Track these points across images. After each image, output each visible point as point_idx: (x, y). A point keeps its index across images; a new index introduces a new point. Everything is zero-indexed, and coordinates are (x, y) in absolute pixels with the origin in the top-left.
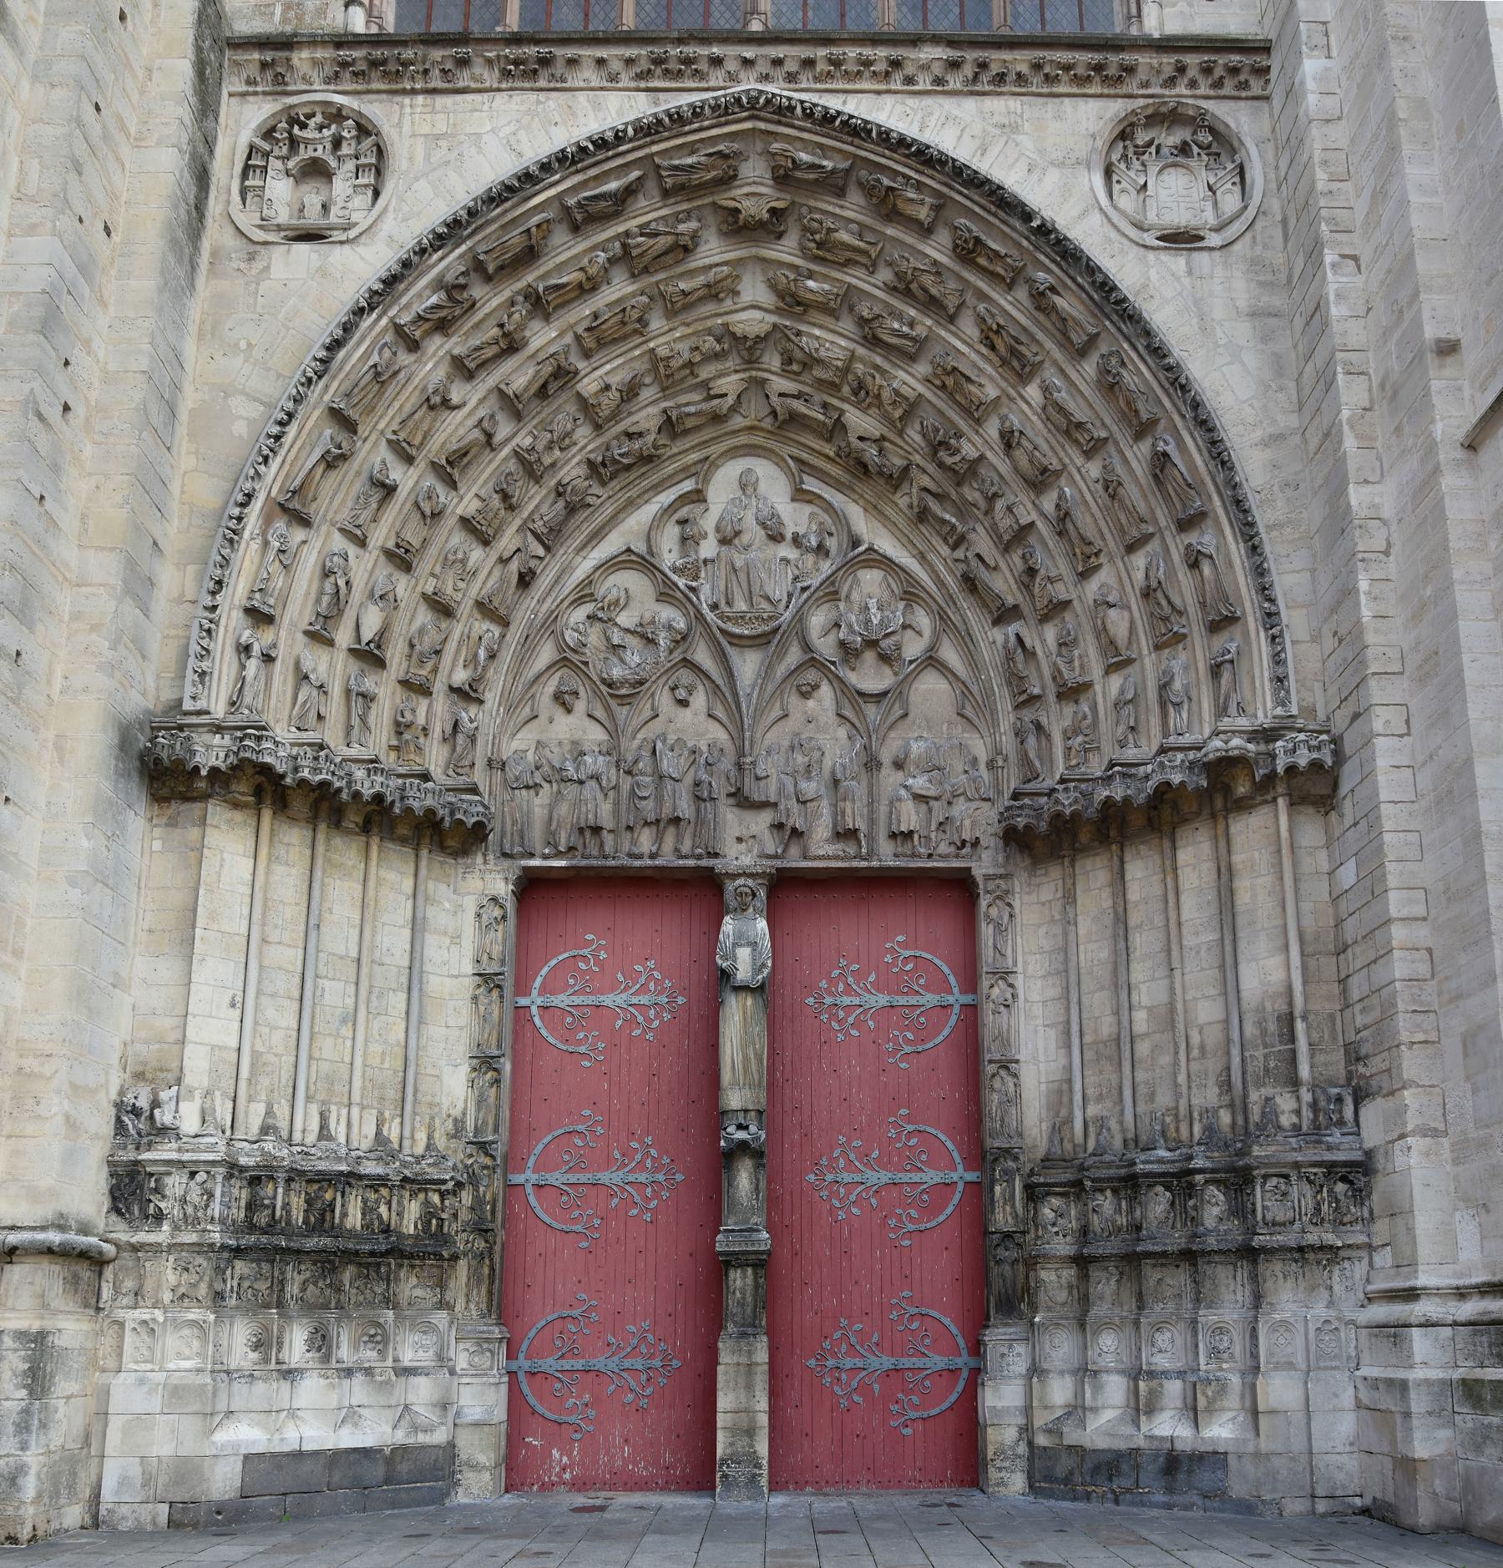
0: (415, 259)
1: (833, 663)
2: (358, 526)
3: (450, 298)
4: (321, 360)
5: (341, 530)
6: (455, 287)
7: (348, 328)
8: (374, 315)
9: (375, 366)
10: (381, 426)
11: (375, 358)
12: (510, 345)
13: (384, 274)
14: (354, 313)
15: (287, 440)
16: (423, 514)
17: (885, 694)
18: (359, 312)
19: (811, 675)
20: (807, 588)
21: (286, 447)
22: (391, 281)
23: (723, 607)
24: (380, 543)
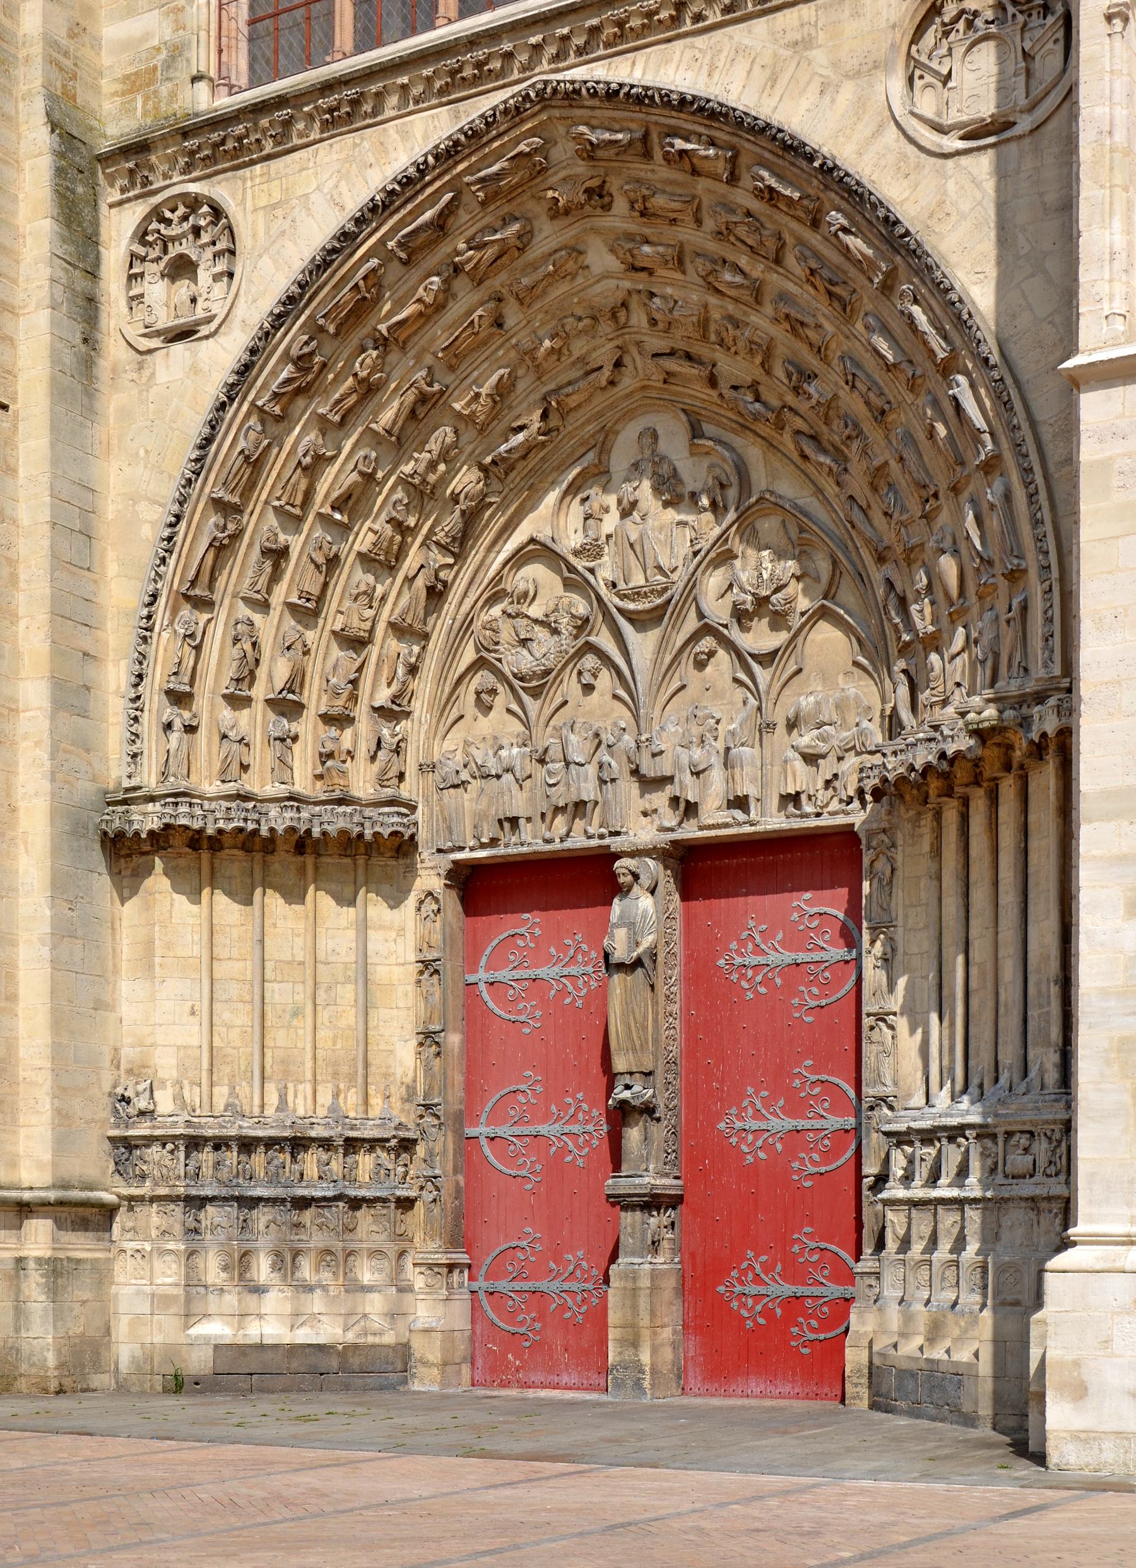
0: (261, 344)
1: (726, 626)
2: (258, 592)
3: (299, 369)
4: (196, 460)
5: (243, 598)
6: (300, 358)
7: (213, 425)
8: (235, 405)
9: (242, 452)
10: (263, 497)
11: (242, 444)
12: (368, 390)
13: (237, 367)
14: (218, 410)
15: (179, 539)
16: (317, 566)
17: (776, 651)
18: (222, 407)
19: (708, 643)
20: (699, 551)
21: (179, 544)
22: (245, 370)
23: (621, 585)
24: (282, 599)
